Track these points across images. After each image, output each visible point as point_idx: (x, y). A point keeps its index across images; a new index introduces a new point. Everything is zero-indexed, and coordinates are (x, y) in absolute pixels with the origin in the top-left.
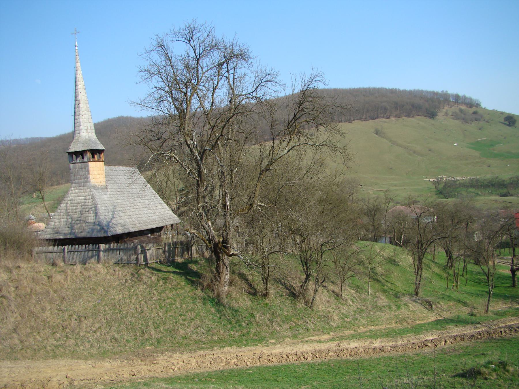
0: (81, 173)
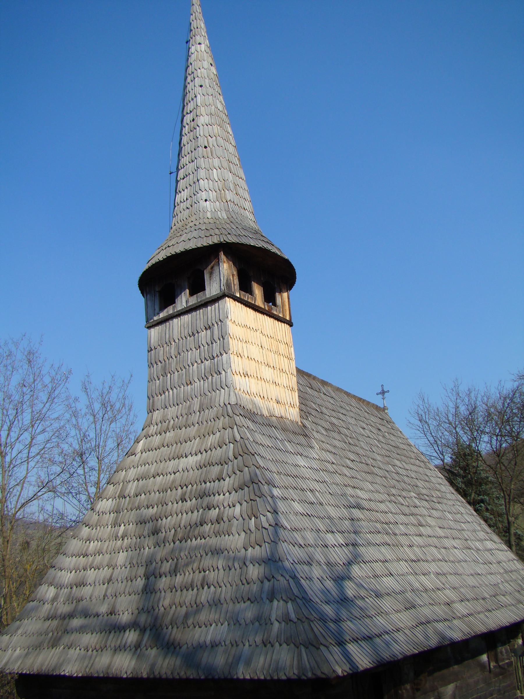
0: (193, 355)
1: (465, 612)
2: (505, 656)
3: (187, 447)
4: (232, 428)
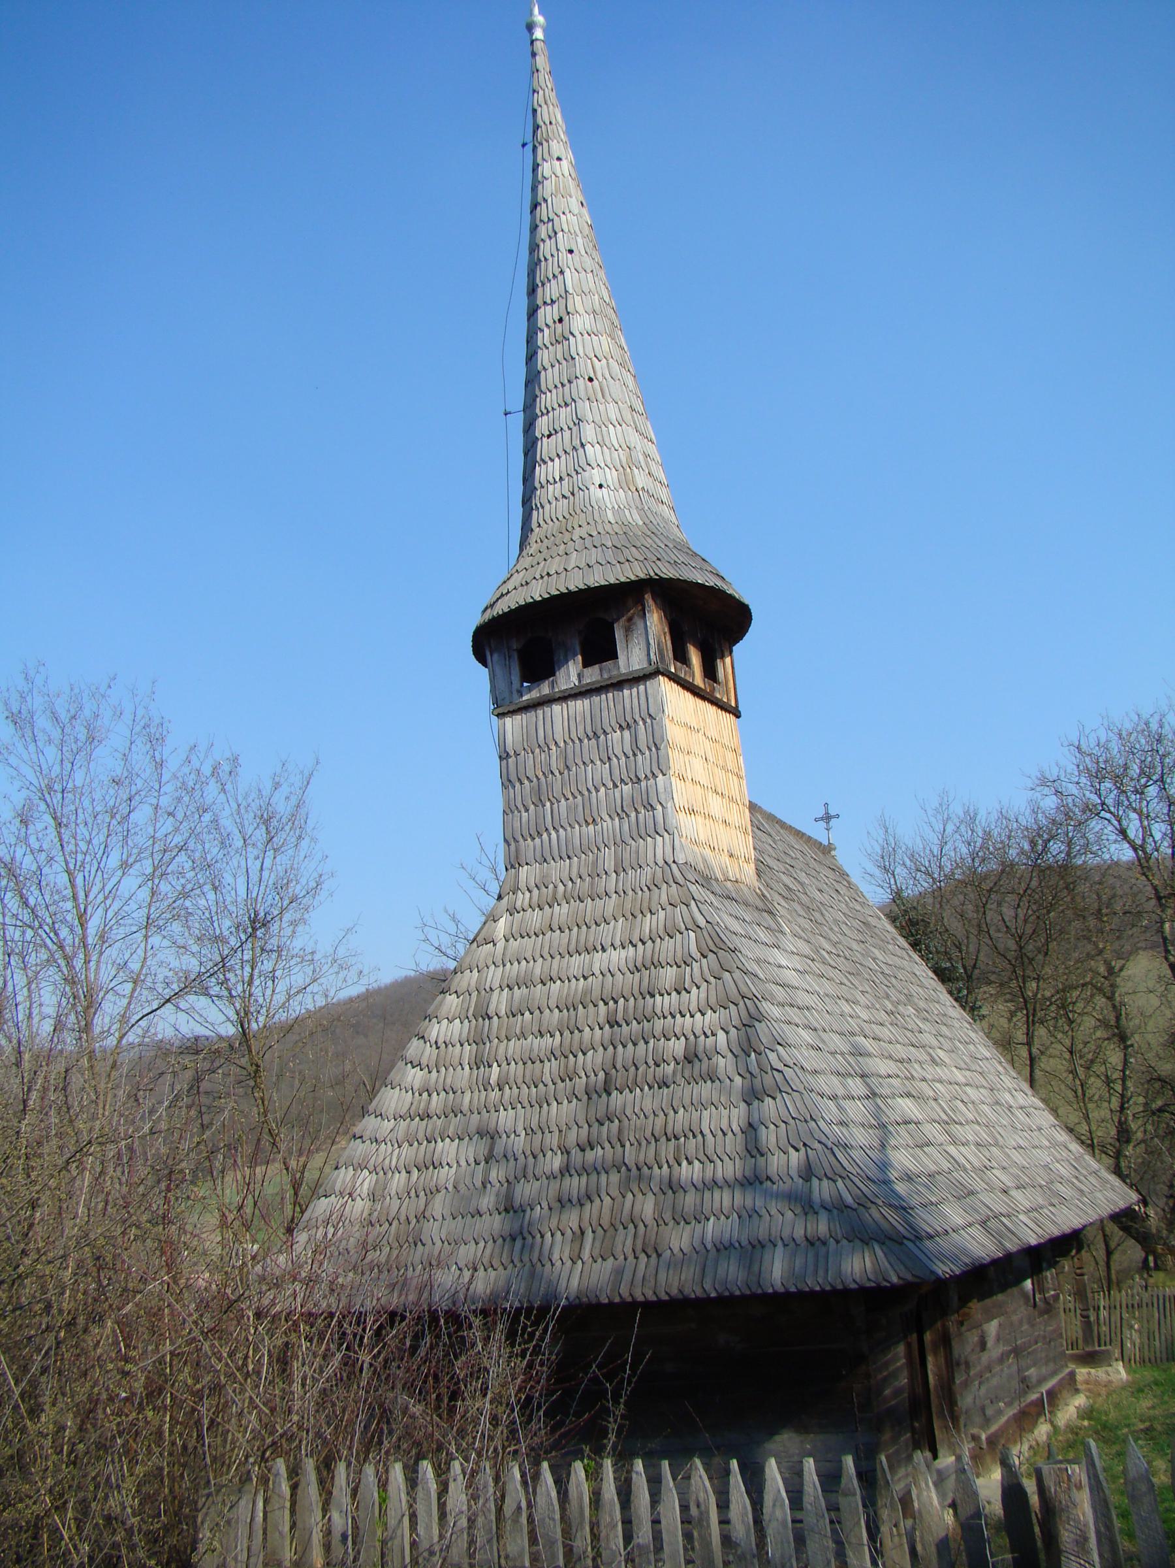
3: (605, 933)
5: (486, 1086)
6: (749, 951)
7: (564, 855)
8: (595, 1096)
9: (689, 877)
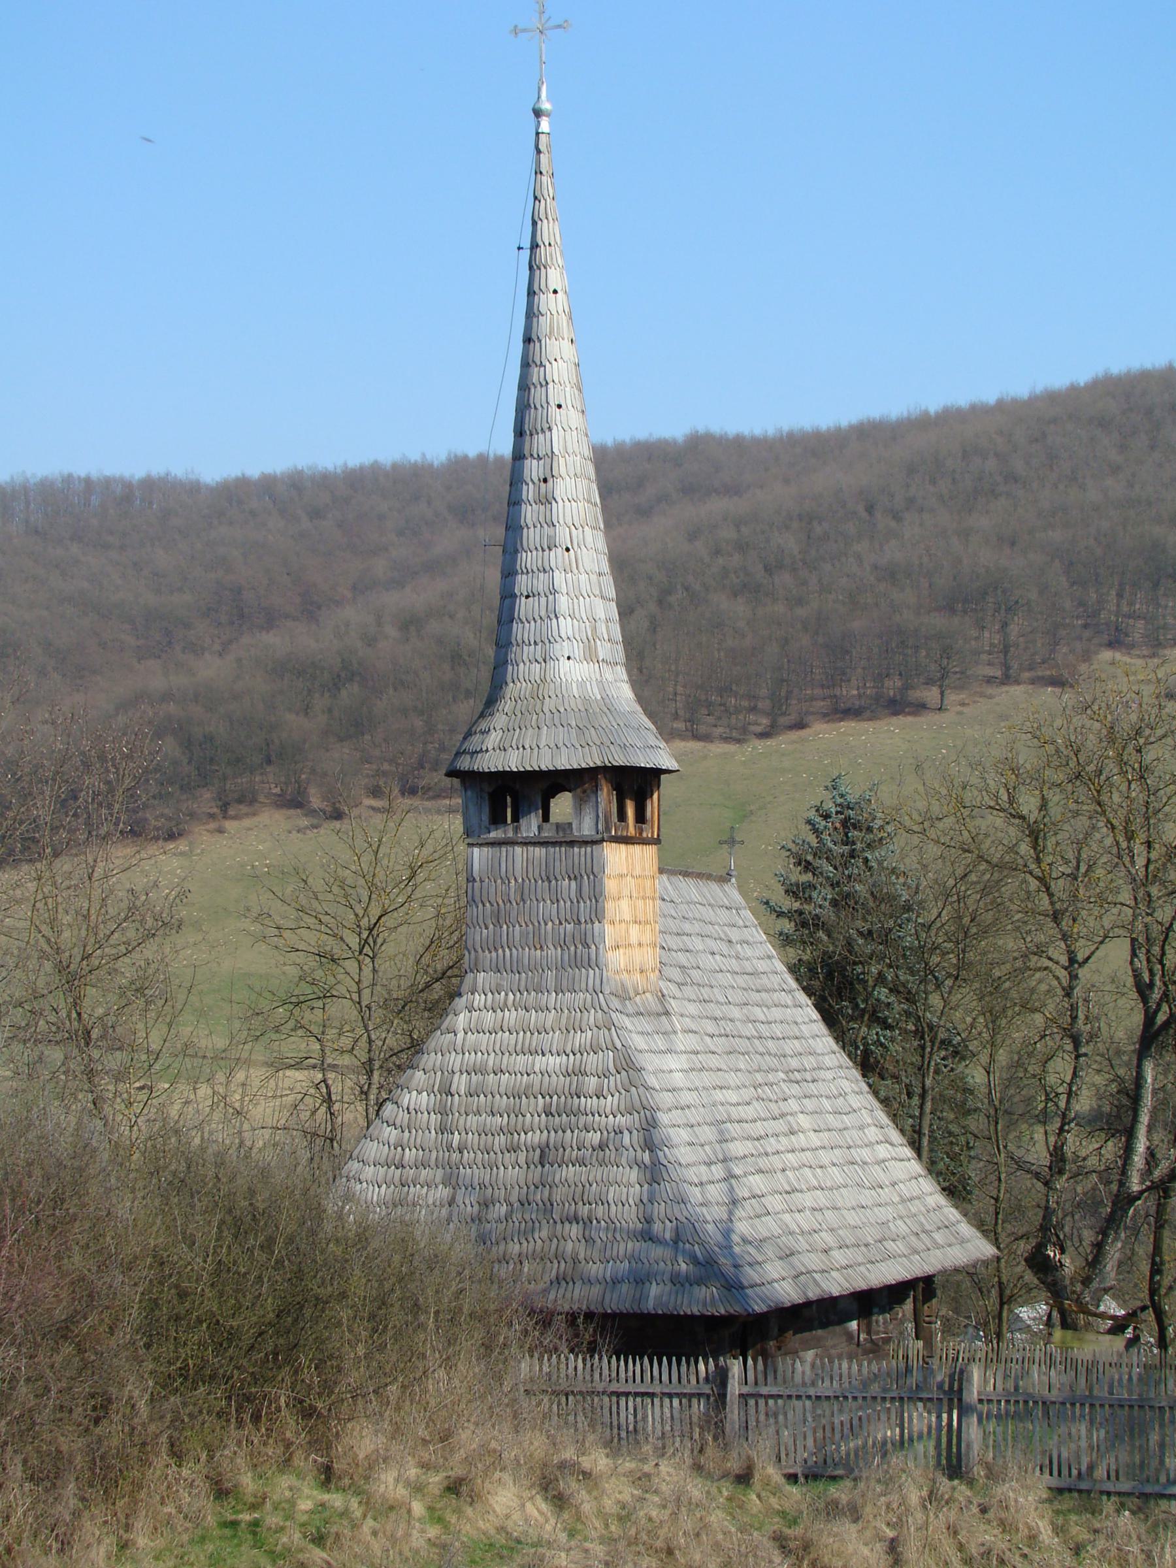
1: (844, 1262)
2: (881, 1329)
4: (609, 1030)
5: (449, 1147)
6: (649, 1062)
7: (515, 970)
8: (532, 1166)
9: (612, 1006)
